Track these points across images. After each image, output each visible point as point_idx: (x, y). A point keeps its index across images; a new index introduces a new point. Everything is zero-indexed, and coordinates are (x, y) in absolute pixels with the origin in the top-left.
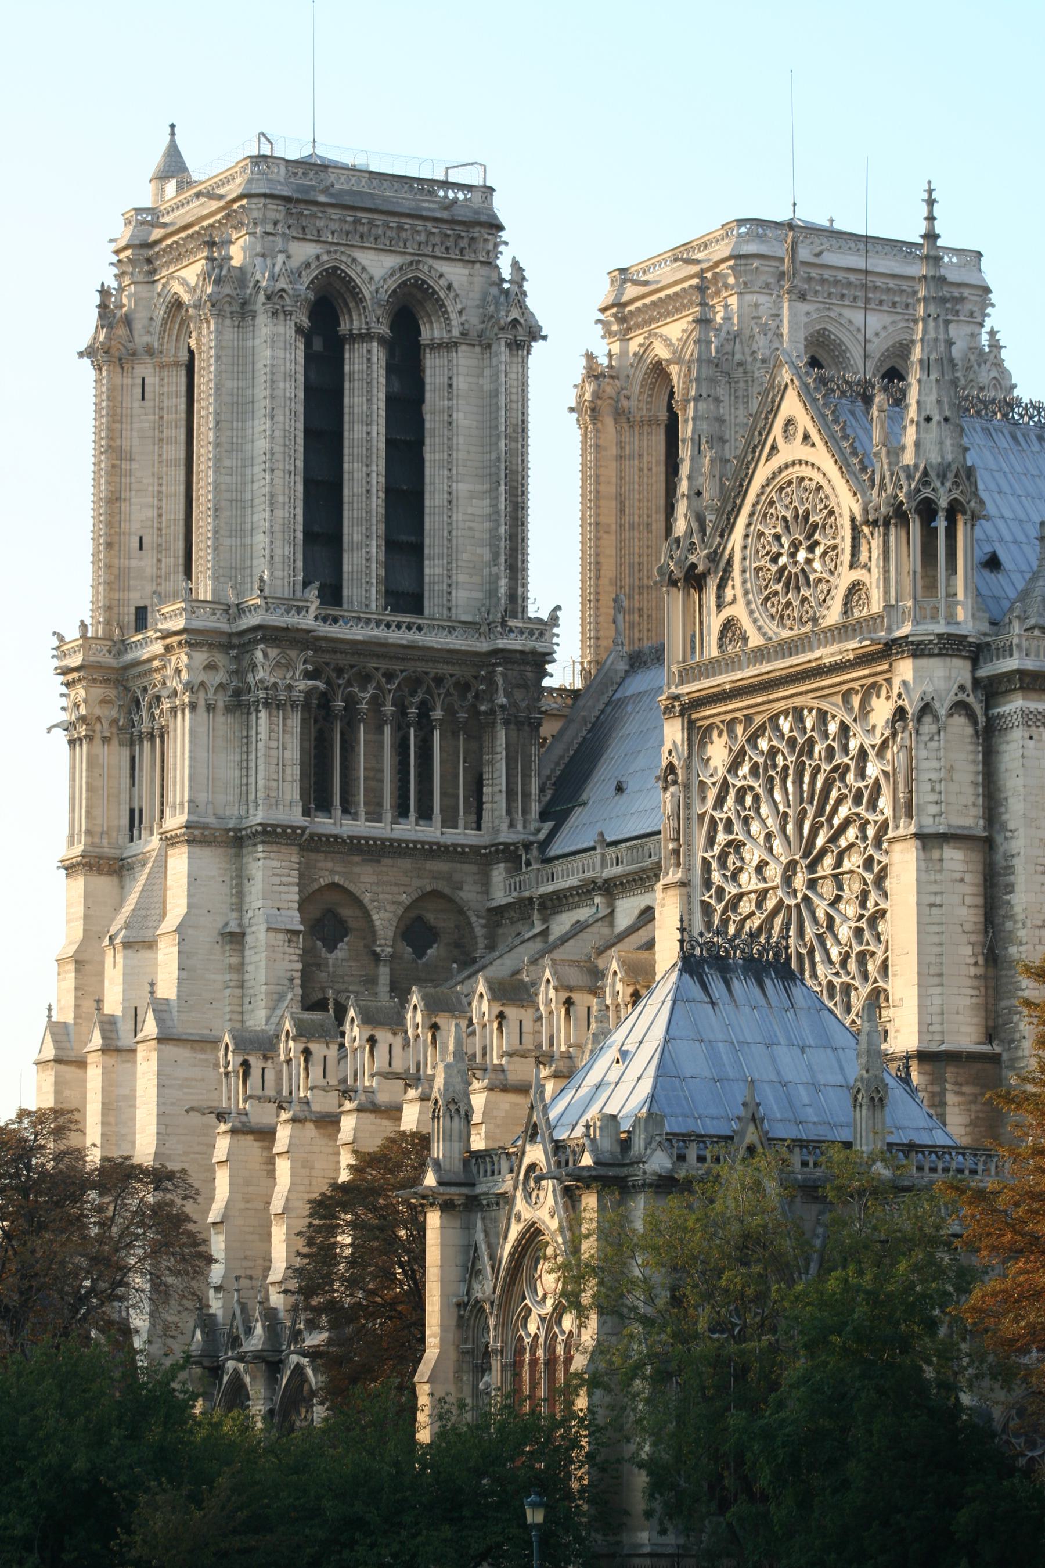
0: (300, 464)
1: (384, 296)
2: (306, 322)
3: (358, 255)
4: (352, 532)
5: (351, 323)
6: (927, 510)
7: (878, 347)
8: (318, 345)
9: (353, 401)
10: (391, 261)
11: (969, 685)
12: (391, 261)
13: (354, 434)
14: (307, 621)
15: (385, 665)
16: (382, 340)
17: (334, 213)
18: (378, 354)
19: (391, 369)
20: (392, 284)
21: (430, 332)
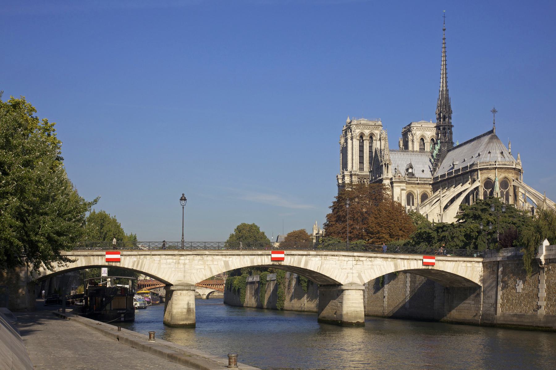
0: (358, 155)
1: (368, 135)
2: (358, 138)
3: (364, 130)
4: (365, 162)
5: (364, 138)
6: (385, 164)
7: (430, 136)
8: (361, 141)
9: (365, 147)
10: (369, 131)
11: (389, 183)
12: (370, 131)
13: (365, 151)
14: (356, 173)
15: (367, 177)
16: (368, 140)
17: (362, 126)
18: (368, 142)
19: (370, 143)
20: (369, 133)
21: (374, 138)
